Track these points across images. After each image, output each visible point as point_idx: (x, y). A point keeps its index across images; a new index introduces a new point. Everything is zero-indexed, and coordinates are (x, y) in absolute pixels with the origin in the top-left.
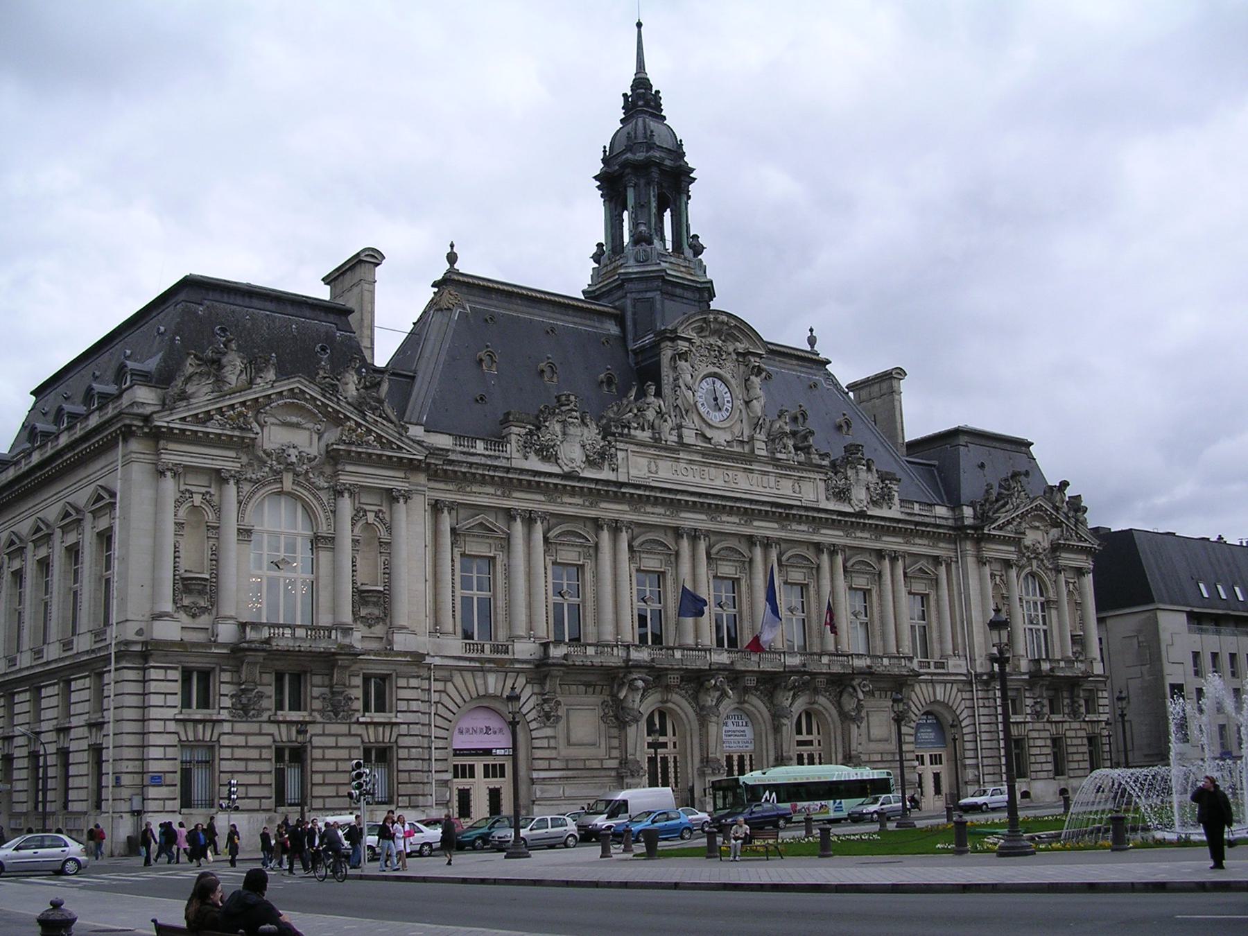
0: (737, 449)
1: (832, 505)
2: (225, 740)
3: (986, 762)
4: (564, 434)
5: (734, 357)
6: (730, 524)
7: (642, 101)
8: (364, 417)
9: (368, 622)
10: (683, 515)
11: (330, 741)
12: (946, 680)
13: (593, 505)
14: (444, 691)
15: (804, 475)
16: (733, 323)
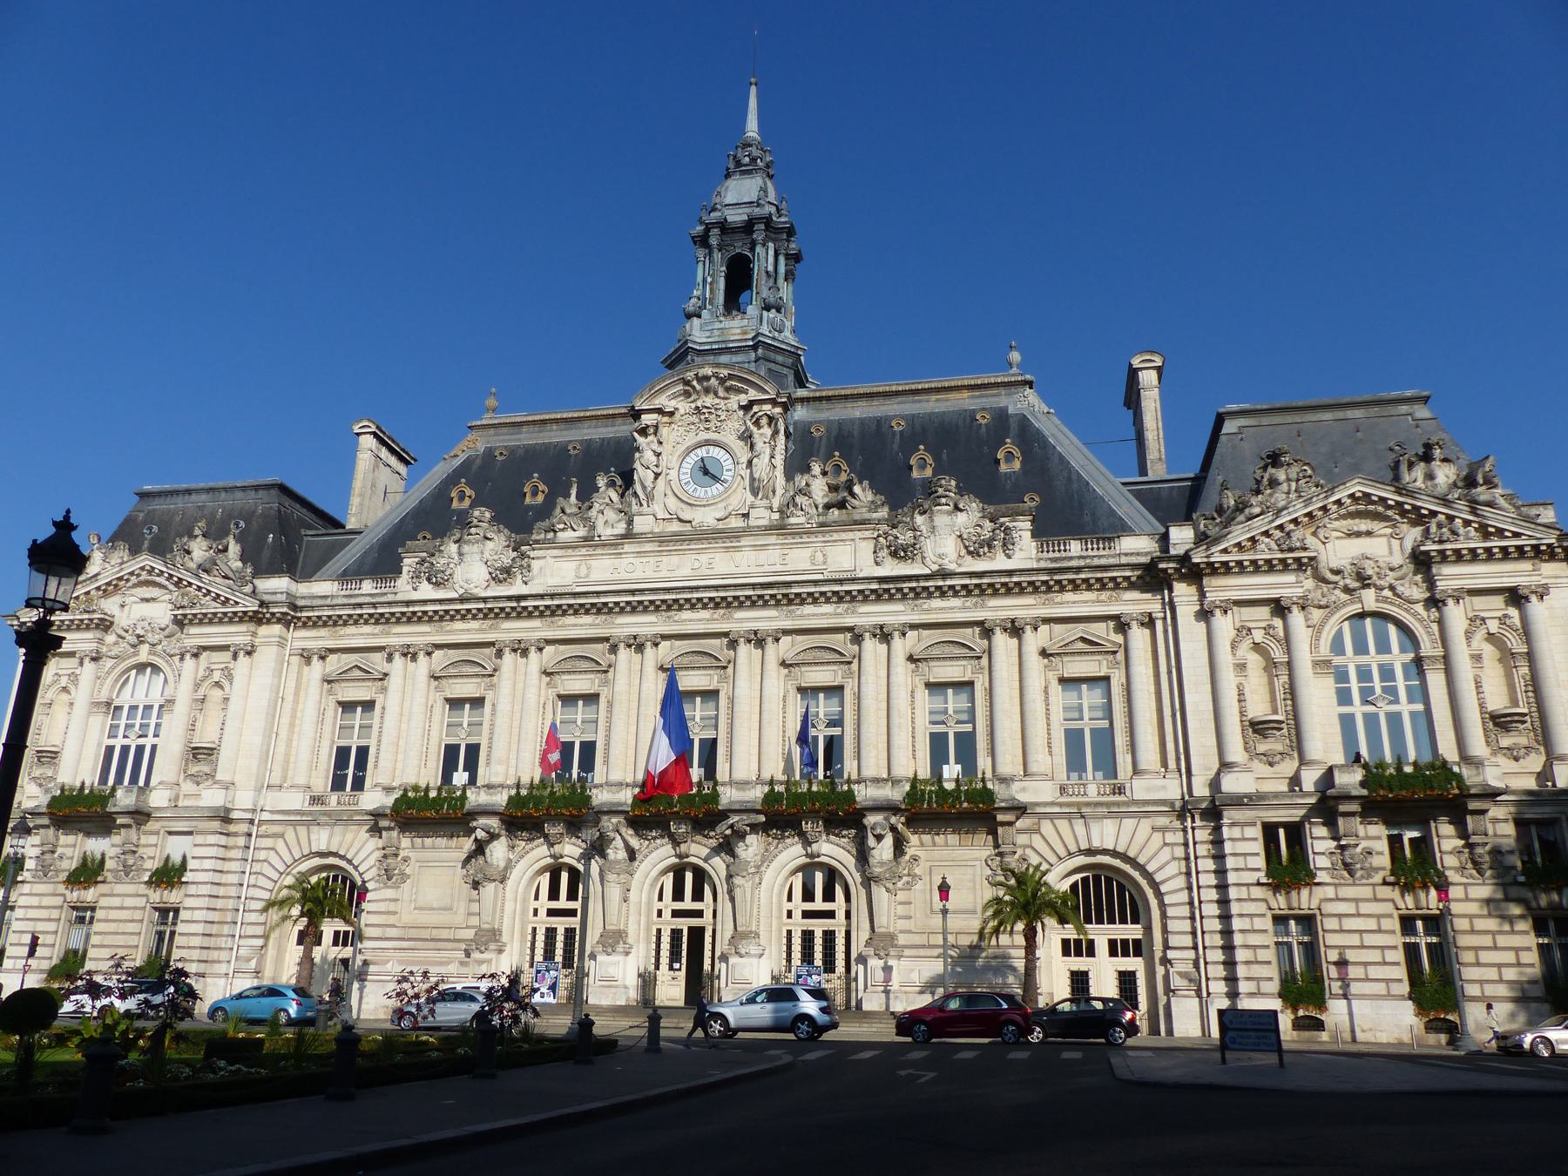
1: (891, 568)
4: (460, 554)
8: (200, 578)
9: (196, 779)
11: (116, 902)
12: (1143, 810)
15: (836, 536)
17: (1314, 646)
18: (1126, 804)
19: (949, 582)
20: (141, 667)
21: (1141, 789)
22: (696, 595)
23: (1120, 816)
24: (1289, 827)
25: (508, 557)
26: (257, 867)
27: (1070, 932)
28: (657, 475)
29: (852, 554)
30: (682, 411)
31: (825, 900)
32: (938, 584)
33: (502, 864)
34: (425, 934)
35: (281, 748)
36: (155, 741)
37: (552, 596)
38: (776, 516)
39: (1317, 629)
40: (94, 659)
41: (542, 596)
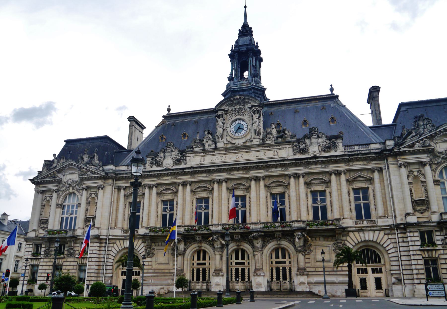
0: (248, 144)
1: (298, 156)
2: (41, 264)
3: (405, 272)
4: (164, 156)
5: (248, 110)
6: (238, 174)
7: (246, 31)
8: (87, 167)
10: (215, 175)
11: (68, 264)
12: (381, 229)
13: (176, 178)
14: (113, 247)
15: (281, 147)
16: (243, 97)
17: (434, 176)
18: (376, 226)
19: (317, 160)
20: (70, 194)
21: (380, 222)
22: (238, 166)
23: (374, 231)
24: (427, 232)
25: (179, 157)
26: (109, 253)
27: (360, 266)
28: (224, 130)
29: (286, 152)
30: (230, 110)
31: (282, 258)
32: (314, 160)
33: (183, 250)
34: (160, 271)
35: (114, 217)
36: (76, 215)
37: (194, 168)
38: (262, 141)
39: (434, 171)
40: (56, 192)
41: (190, 168)
